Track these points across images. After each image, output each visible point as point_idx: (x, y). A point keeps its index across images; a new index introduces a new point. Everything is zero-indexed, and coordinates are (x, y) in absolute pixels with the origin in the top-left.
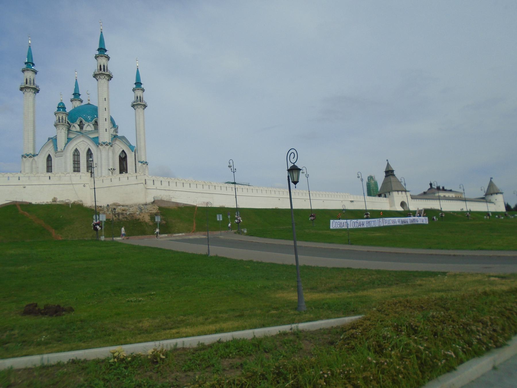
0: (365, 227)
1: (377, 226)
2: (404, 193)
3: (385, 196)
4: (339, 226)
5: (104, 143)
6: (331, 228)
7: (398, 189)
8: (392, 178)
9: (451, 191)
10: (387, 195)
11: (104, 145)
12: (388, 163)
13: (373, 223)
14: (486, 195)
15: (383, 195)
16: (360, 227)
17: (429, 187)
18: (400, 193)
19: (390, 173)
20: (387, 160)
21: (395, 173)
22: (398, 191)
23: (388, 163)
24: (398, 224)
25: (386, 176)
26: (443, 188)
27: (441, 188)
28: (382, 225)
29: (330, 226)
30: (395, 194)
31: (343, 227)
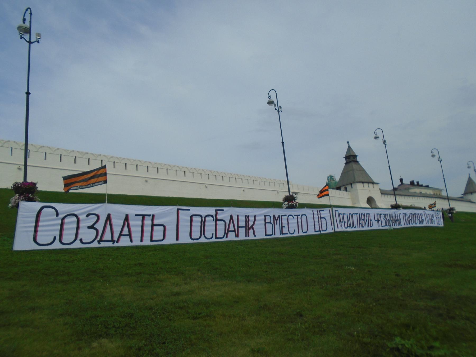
0: (260, 235)
1: (311, 232)
2: (371, 185)
3: (346, 190)
4: (87, 235)
6: (23, 241)
7: (364, 181)
8: (354, 165)
9: (427, 186)
10: (349, 187)
12: (349, 147)
13: (293, 221)
14: (465, 194)
15: (342, 188)
16: (231, 237)
17: (400, 183)
18: (366, 185)
19: (352, 159)
20: (348, 142)
21: (358, 159)
22: (363, 183)
23: (349, 147)
24: (375, 226)
25: (346, 163)
26: (418, 183)
27: (416, 183)
28: (330, 230)
29: (12, 237)
30: (359, 186)
31: (124, 242)
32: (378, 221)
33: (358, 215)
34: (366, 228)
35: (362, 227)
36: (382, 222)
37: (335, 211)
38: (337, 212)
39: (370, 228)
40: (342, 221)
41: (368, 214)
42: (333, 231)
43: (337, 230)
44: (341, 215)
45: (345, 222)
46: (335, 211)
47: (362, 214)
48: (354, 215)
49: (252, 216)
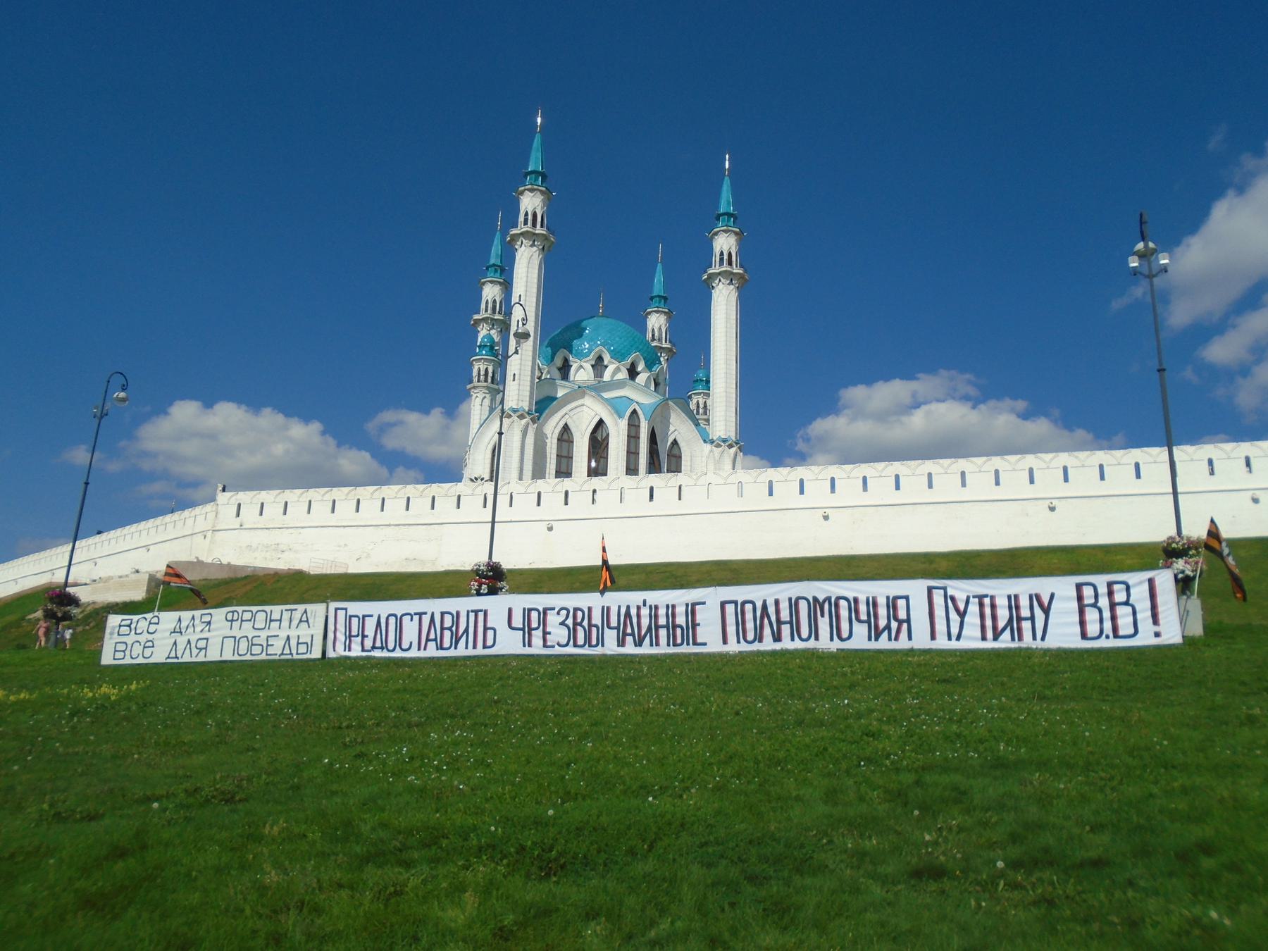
5: (515, 411)
11: (515, 417)
32: (527, 630)
33: (426, 619)
34: (461, 651)
35: (440, 647)
36: (545, 633)
37: (336, 609)
38: (341, 614)
39: (480, 651)
40: (354, 632)
41: (476, 612)
42: (316, 654)
43: (331, 654)
44: (355, 621)
45: (364, 636)
46: (336, 609)
47: (443, 614)
48: (406, 619)
49: (680, 605)
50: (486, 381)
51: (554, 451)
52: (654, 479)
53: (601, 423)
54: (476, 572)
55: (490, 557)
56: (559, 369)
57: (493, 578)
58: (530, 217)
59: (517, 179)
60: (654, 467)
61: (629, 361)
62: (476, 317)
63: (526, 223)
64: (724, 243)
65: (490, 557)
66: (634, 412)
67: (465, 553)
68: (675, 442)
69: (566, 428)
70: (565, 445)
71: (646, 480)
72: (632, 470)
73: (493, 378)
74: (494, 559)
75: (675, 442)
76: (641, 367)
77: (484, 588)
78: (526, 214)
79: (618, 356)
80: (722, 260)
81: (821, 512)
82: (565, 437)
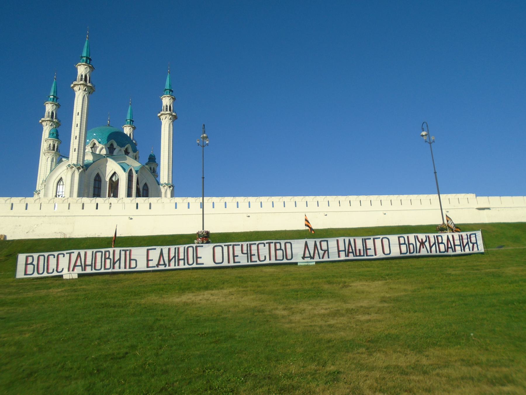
50: (53, 150)
51: (93, 185)
52: (140, 200)
53: (115, 173)
54: (198, 233)
55: (203, 229)
56: (91, 148)
57: (207, 237)
58: (84, 77)
59: (78, 60)
60: (138, 195)
61: (126, 147)
62: (43, 119)
63: (81, 80)
64: (166, 101)
65: (203, 229)
66: (131, 170)
67: (192, 227)
68: (146, 185)
69: (98, 175)
70: (97, 182)
71: (135, 200)
72: (129, 195)
73: (57, 149)
74: (206, 229)
75: (146, 185)
76: (130, 150)
77: (205, 242)
78: (82, 76)
79: (121, 145)
80: (167, 109)
81: (245, 215)
82: (97, 179)
